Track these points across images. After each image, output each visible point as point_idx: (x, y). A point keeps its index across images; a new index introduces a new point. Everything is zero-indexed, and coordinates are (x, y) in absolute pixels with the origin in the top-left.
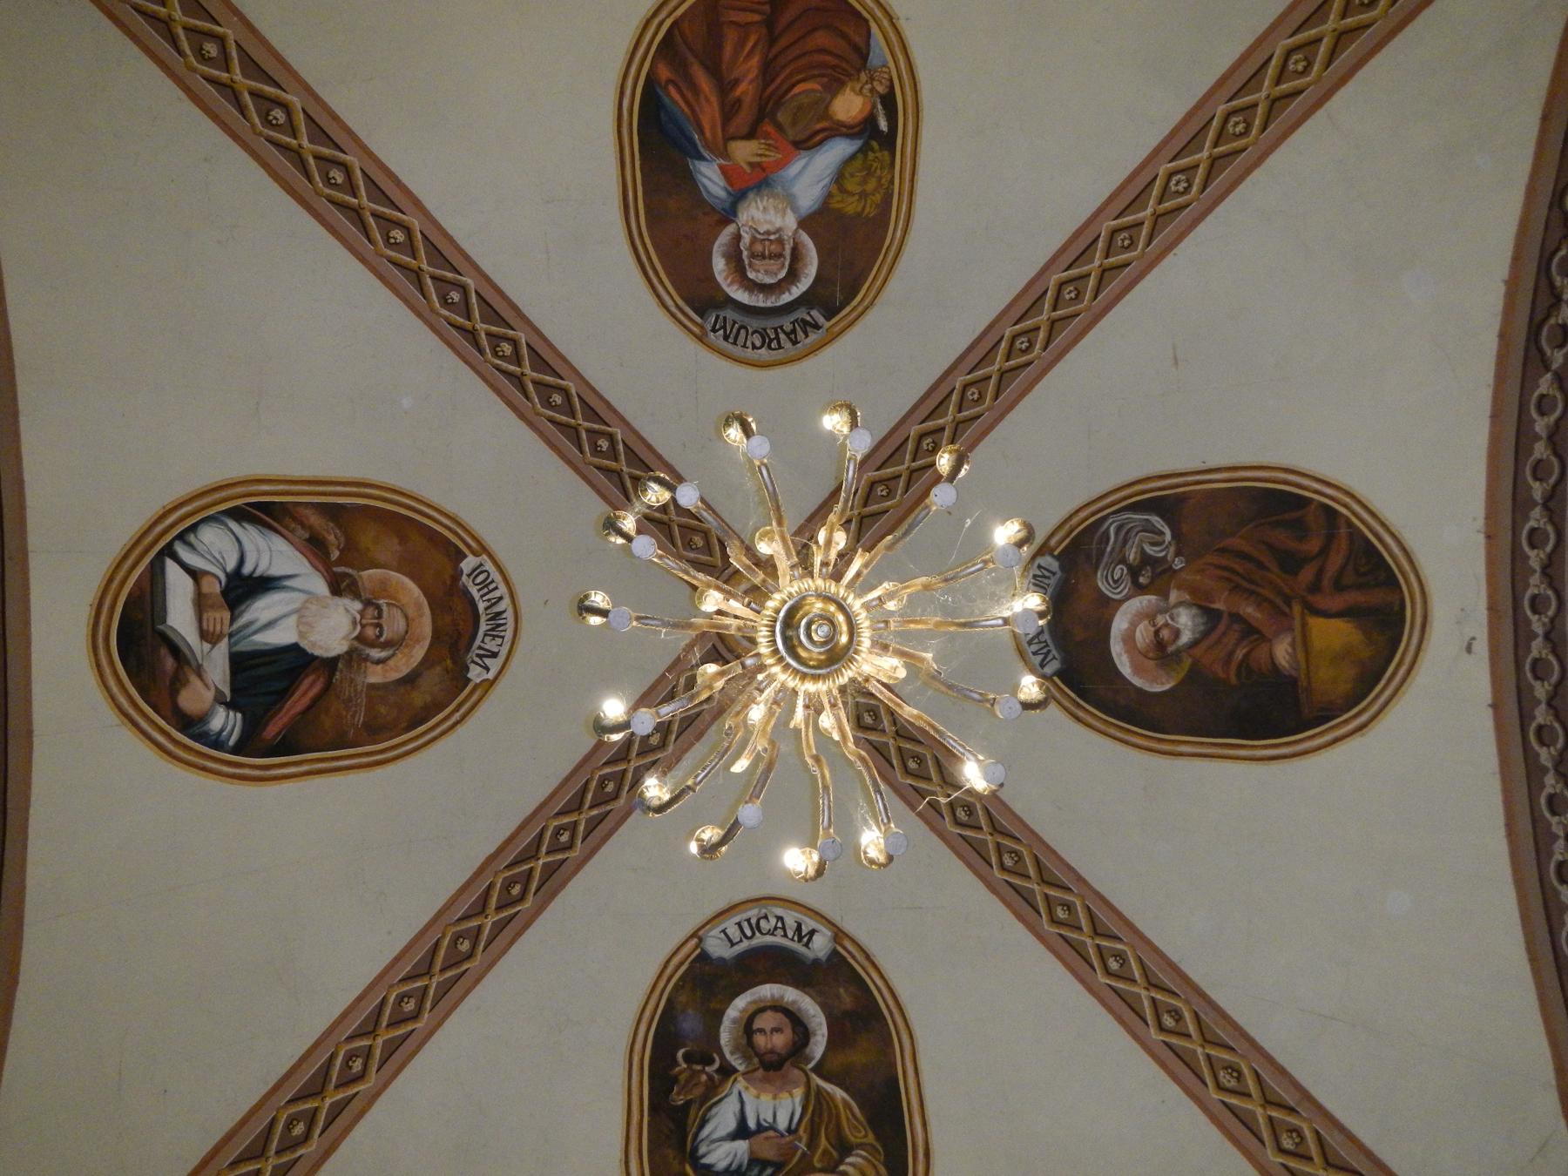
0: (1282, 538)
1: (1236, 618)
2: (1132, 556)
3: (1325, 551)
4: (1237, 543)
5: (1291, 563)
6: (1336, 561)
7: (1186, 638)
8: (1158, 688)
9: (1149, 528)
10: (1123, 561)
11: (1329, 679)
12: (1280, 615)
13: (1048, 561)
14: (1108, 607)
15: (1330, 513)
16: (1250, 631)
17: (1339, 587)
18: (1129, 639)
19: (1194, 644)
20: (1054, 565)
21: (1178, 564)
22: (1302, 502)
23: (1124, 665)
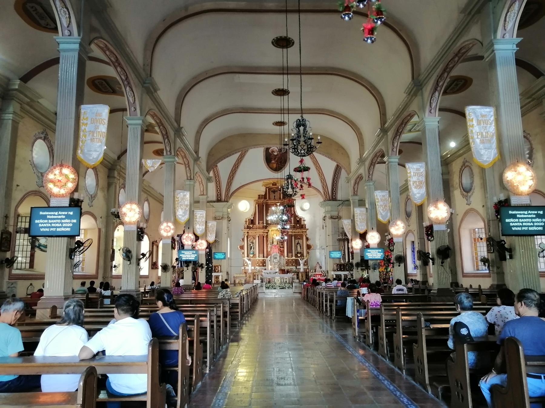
1: (276, 158)
5: (281, 162)
11: (271, 165)
12: (277, 161)
16: (275, 159)
17: (278, 166)
18: (274, 149)
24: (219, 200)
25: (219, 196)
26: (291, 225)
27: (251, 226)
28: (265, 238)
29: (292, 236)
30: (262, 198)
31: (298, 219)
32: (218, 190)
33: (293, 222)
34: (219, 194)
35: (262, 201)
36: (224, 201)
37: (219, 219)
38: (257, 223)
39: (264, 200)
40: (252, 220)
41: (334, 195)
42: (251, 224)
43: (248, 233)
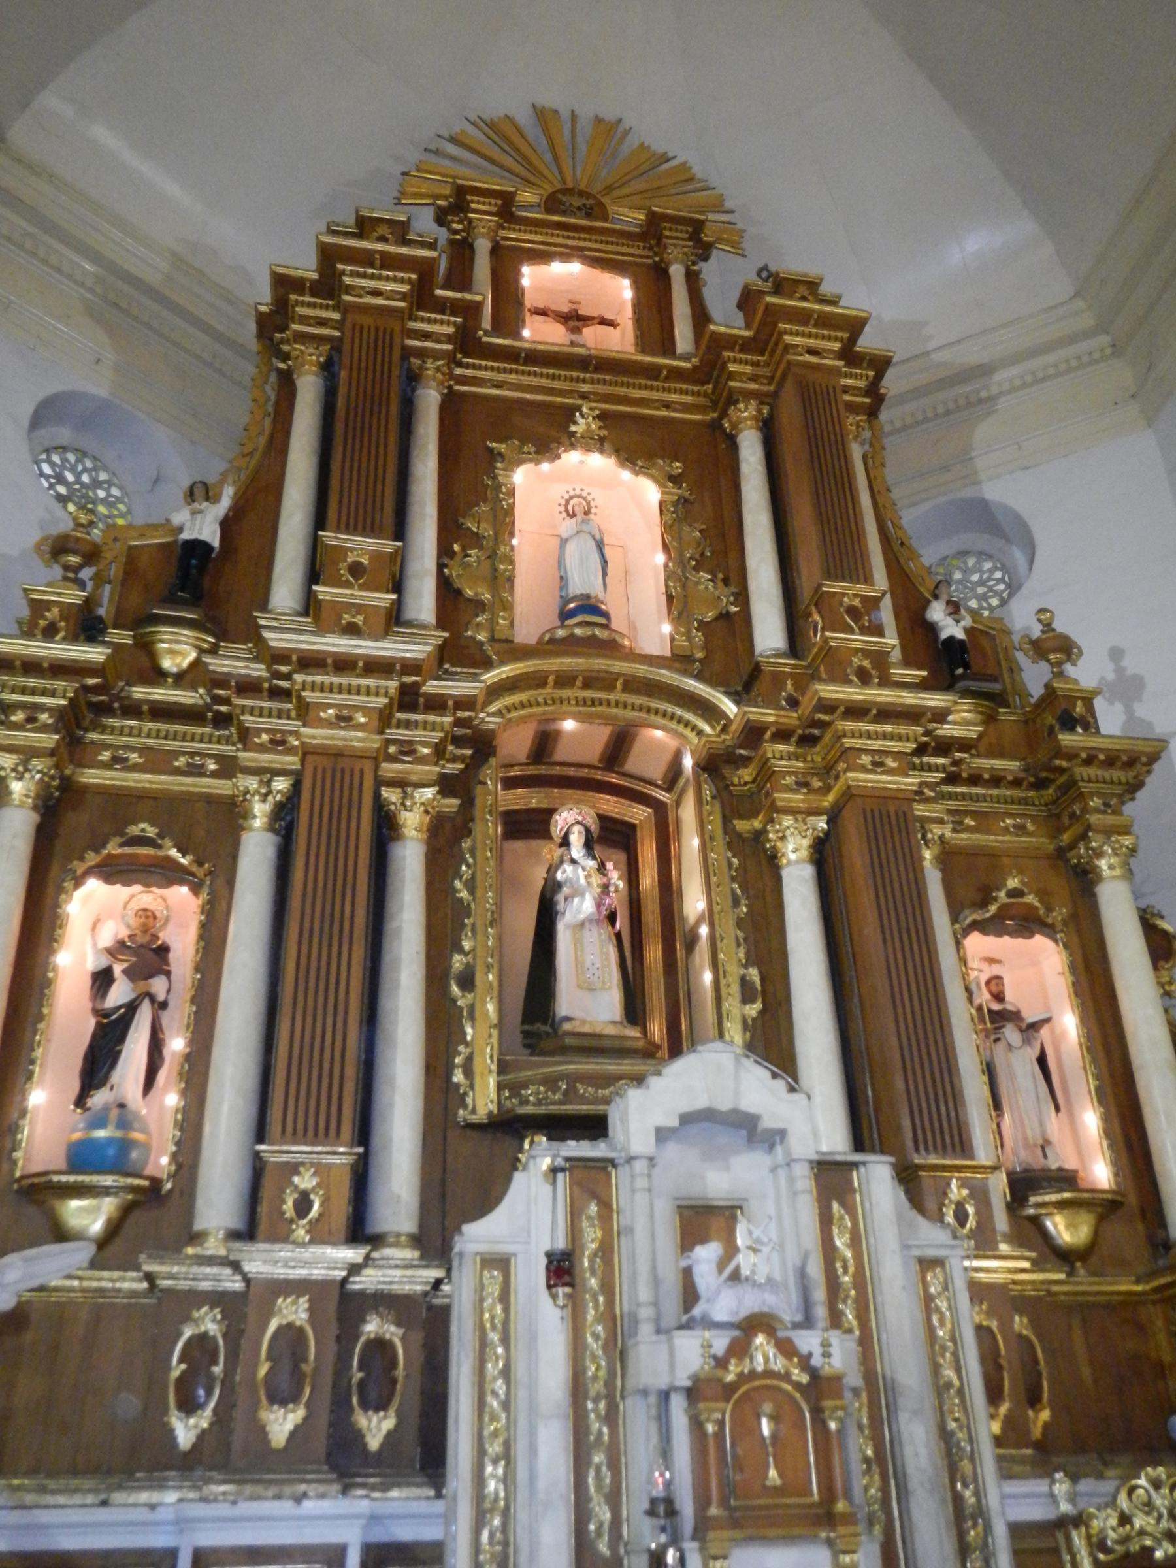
31: (952, 629)
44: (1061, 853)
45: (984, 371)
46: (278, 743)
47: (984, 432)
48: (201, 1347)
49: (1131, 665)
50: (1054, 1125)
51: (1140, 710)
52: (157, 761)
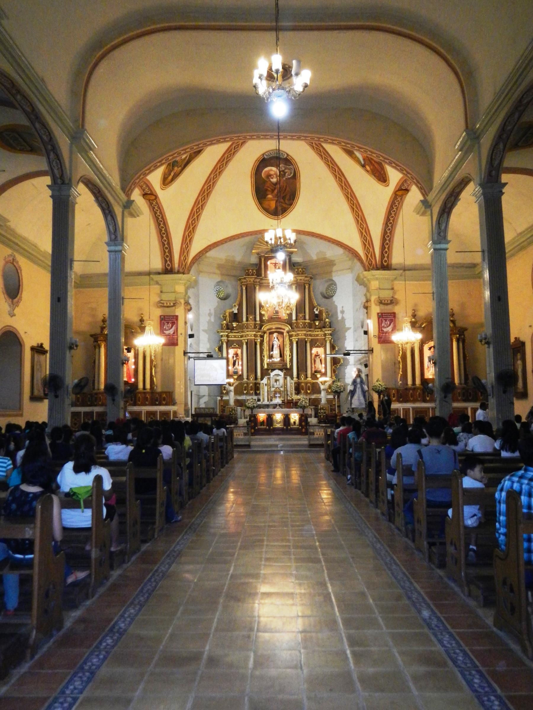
0: (288, 197)
1: (275, 189)
2: (286, 171)
3: (286, 204)
4: (288, 188)
5: (284, 198)
6: (284, 205)
7: (272, 180)
8: (263, 175)
9: (291, 173)
10: (285, 169)
11: (266, 204)
12: (277, 196)
13: (286, 156)
14: (277, 166)
15: (291, 204)
16: (273, 191)
19: (270, 181)
20: (285, 157)
21: (284, 179)
22: (293, 200)
23: (266, 169)
24: (168, 270)
25: (169, 262)
26: (305, 323)
27: (235, 324)
28: (258, 346)
29: (306, 342)
30: (253, 275)
31: (317, 312)
32: (167, 251)
33: (307, 317)
34: (168, 259)
35: (252, 280)
36: (178, 272)
37: (168, 307)
38: (244, 319)
39: (255, 278)
40: (235, 314)
41: (386, 259)
42: (234, 321)
43: (228, 336)
44: (325, 339)
45: (334, 261)
46: (246, 337)
47: (335, 268)
48: (245, 387)
49: (344, 309)
50: (320, 366)
51: (344, 316)
52: (235, 337)
